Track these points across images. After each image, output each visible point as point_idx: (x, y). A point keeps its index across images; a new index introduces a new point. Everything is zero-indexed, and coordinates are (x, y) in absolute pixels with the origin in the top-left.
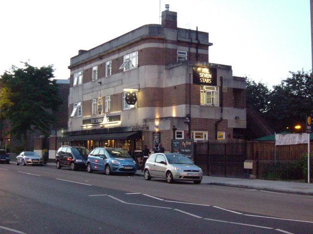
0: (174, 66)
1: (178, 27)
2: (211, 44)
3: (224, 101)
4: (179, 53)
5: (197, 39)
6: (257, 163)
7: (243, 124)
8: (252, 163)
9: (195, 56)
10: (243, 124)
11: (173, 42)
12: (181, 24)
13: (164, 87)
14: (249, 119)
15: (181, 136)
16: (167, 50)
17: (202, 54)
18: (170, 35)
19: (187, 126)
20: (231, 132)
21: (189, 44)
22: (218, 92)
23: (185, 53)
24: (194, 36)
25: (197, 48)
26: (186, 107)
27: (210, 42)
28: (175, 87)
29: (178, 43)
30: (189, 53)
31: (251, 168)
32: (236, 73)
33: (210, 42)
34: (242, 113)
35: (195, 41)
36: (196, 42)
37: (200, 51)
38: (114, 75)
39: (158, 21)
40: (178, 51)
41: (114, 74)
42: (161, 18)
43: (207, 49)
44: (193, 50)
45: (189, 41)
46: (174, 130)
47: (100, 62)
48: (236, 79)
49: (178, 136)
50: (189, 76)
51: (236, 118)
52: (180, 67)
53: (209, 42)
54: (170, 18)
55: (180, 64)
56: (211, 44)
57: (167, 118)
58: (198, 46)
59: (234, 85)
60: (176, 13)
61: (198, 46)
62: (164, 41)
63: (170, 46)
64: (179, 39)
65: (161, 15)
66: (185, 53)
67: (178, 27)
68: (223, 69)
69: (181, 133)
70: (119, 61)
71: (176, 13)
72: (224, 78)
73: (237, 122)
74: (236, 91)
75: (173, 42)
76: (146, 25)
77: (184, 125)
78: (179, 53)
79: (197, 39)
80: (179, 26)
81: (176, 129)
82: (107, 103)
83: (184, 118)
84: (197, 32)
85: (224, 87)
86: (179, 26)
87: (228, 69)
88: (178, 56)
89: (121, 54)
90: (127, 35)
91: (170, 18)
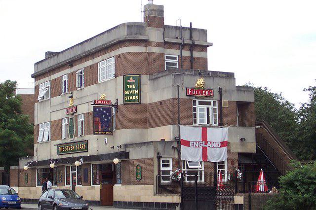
0: (160, 75)
1: (165, 24)
2: (210, 45)
3: (224, 118)
4: (168, 58)
5: (191, 38)
6: (250, 196)
7: (251, 148)
8: (243, 197)
9: (189, 60)
10: (251, 148)
11: (159, 45)
12: (169, 20)
13: (148, 103)
14: (259, 138)
15: (168, 166)
16: (149, 55)
17: (199, 58)
18: (154, 35)
19: (176, 153)
20: (236, 159)
21: (181, 46)
22: (217, 107)
23: (175, 58)
24: (186, 35)
25: (191, 51)
26: (174, 127)
27: (209, 41)
28: (161, 103)
29: (166, 44)
30: (181, 57)
31: (242, 203)
32: (240, 82)
33: (209, 41)
34: (250, 134)
35: (188, 42)
36: (191, 42)
37: (196, 54)
38: (87, 88)
39: (138, 18)
40: (165, 56)
41: (88, 86)
42: (143, 13)
43: (206, 51)
44: (186, 53)
45: (180, 41)
46: (159, 157)
47: (69, 71)
48: (239, 88)
49: (164, 166)
50: (177, 87)
51: (241, 139)
52: (166, 77)
53: (208, 42)
54: (155, 16)
55: (165, 74)
56: (210, 45)
57: (149, 143)
58: (193, 47)
59: (237, 97)
60: (162, 7)
61: (193, 47)
62: (146, 42)
63: (155, 50)
64: (166, 40)
65: (143, 11)
66: (175, 58)
67: (165, 24)
68: (223, 77)
69: (168, 161)
70: (94, 69)
71: (162, 7)
72: (223, 89)
73: (242, 145)
74: (242, 106)
75: (159, 45)
76: (124, 24)
77: (172, 151)
78: (168, 58)
79: (191, 38)
80: (166, 23)
81: (161, 157)
82: (64, 127)
83: (171, 142)
84: (191, 30)
85: (224, 100)
86: (166, 23)
87: (230, 76)
88: (165, 62)
89: (96, 60)
90: (64, 53)
91: (155, 16)
